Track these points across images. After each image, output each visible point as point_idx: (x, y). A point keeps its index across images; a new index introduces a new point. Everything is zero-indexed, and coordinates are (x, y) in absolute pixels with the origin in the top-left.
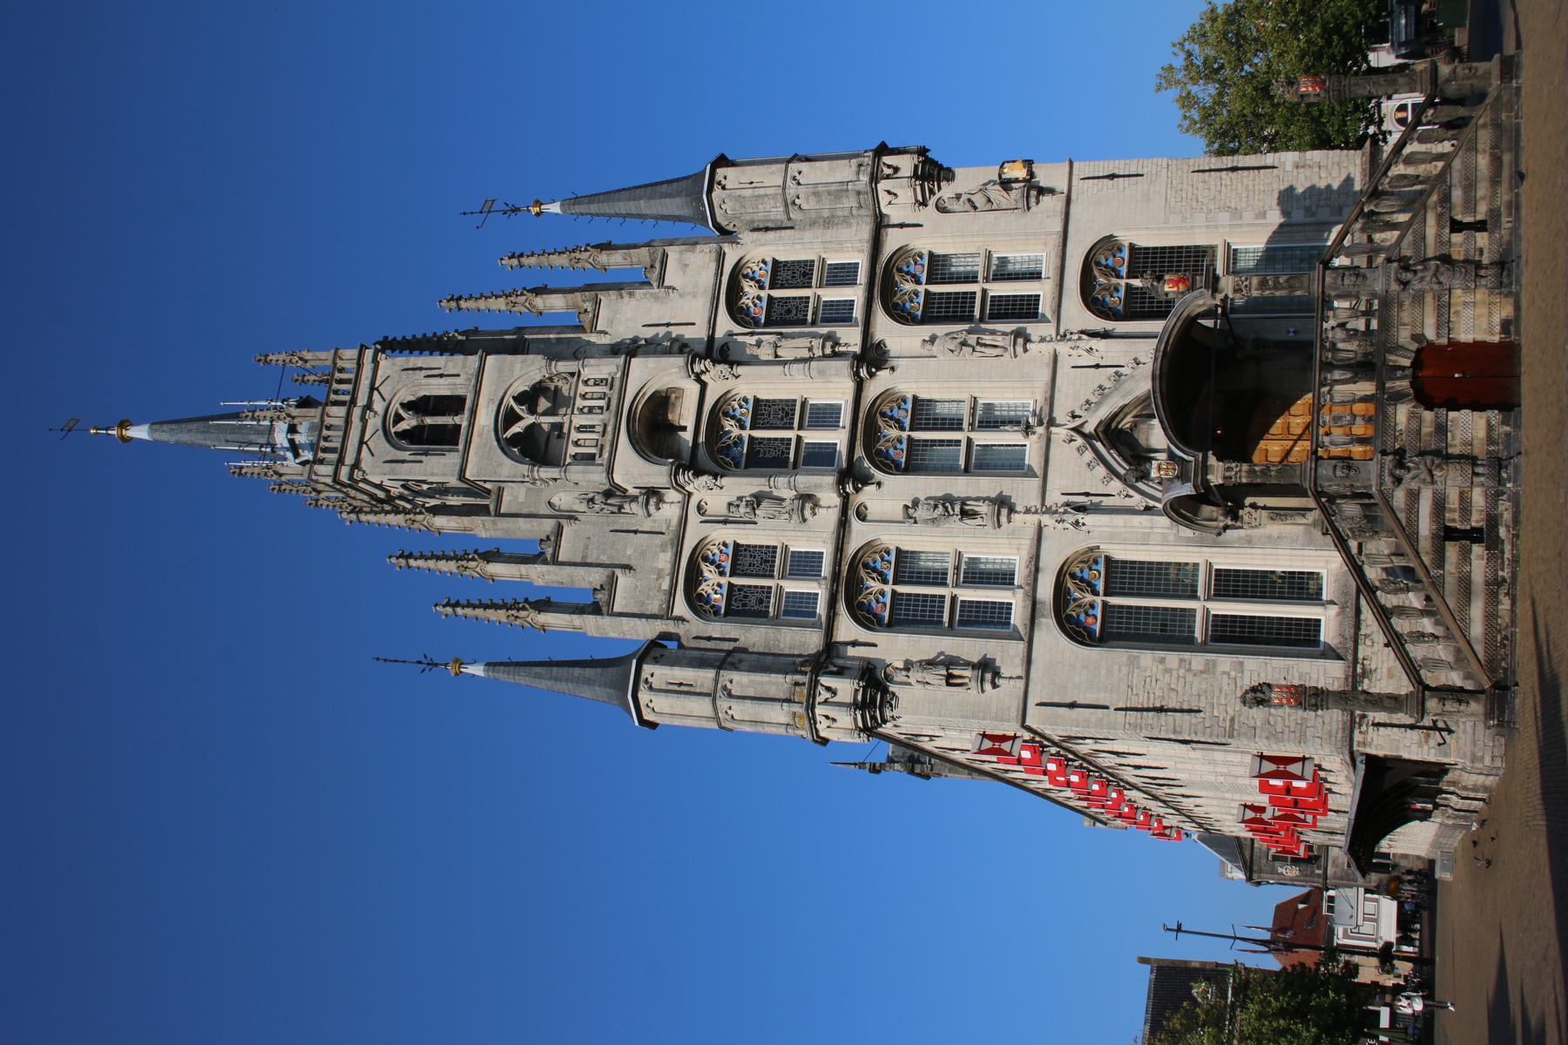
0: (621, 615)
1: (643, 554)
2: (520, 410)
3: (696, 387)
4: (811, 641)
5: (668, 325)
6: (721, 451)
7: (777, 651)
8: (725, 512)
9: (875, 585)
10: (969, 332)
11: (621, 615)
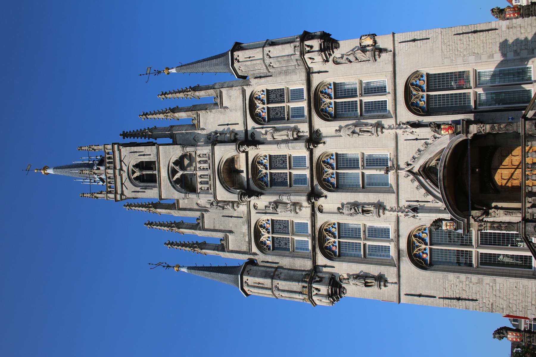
1: (236, 226)
4: (308, 265)
5: (228, 125)
6: (259, 179)
7: (295, 268)
8: (264, 208)
10: (355, 125)
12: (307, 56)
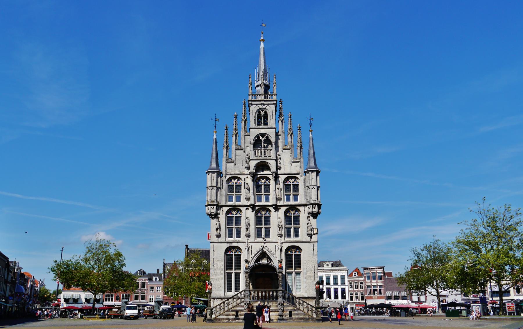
2: (265, 138)
3: (270, 173)
12: (311, 206)
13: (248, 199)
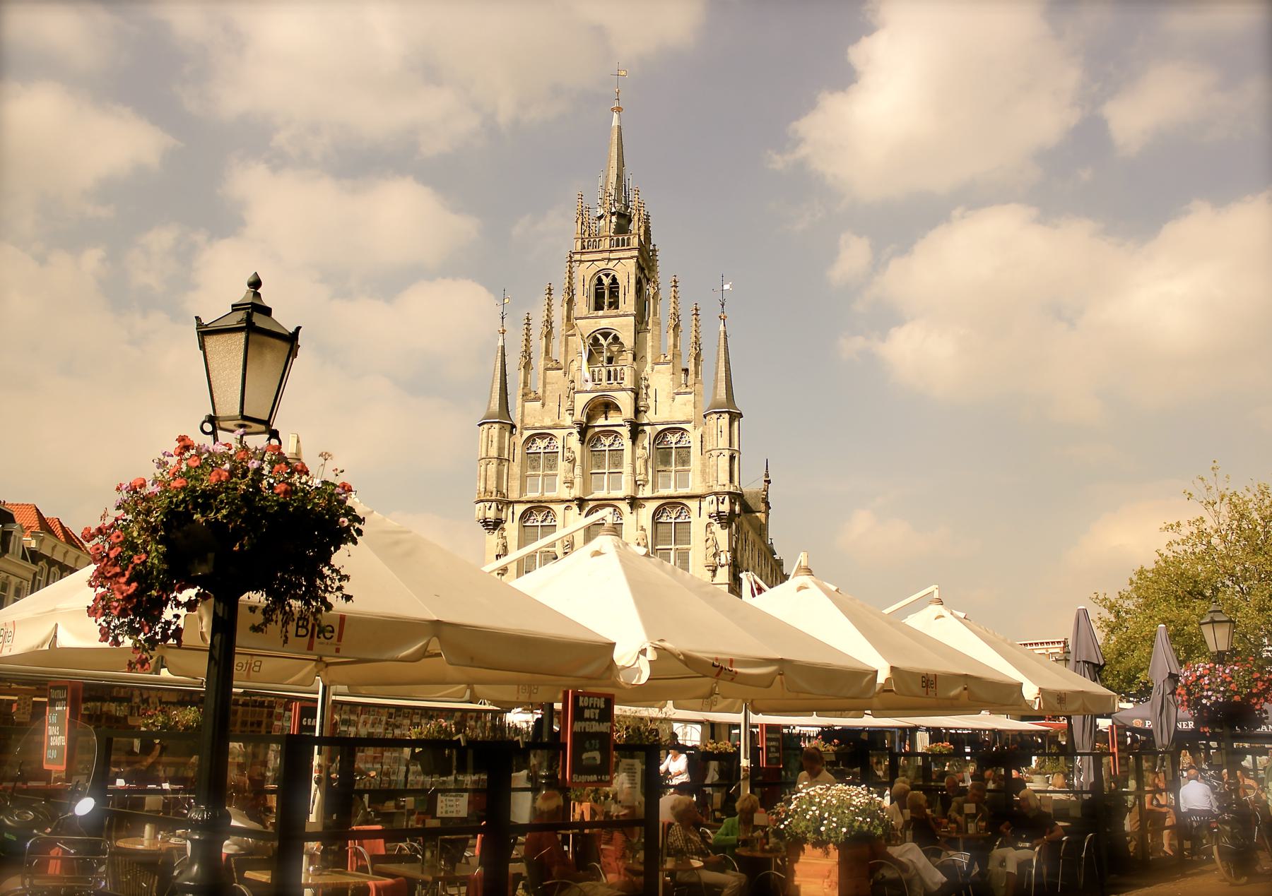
0: (523, 406)
9: (540, 519)
11: (523, 406)
12: (714, 498)
13: (570, 484)
